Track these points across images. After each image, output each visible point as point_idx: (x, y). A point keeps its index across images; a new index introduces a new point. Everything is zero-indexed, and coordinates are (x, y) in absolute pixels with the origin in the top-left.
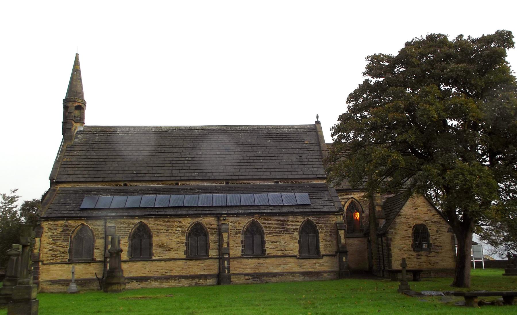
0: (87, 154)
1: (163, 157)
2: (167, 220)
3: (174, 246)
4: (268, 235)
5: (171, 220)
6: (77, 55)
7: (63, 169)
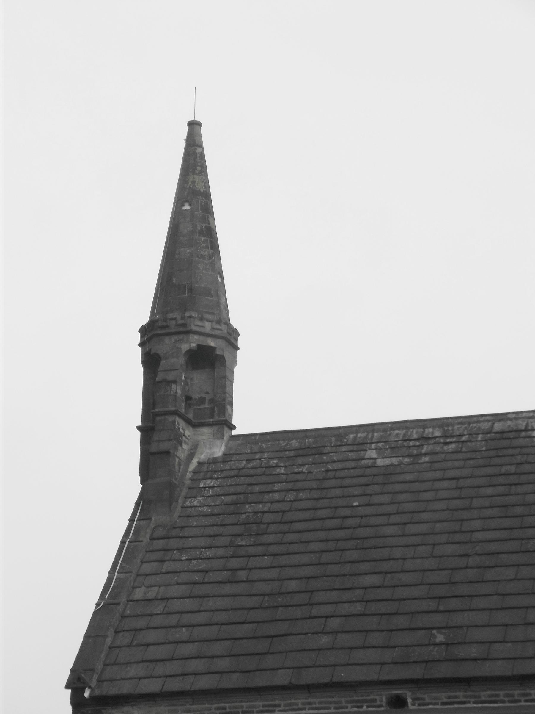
0: (234, 563)
6: (194, 126)
7: (124, 639)
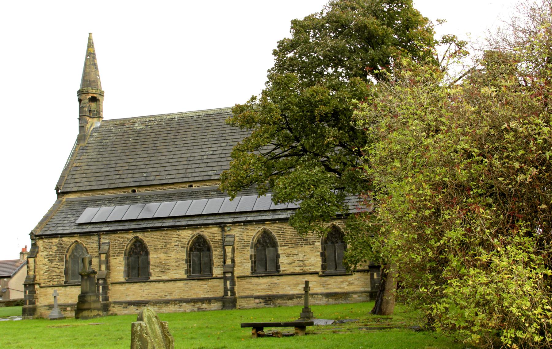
0: (99, 156)
1: (180, 152)
2: (164, 233)
3: (174, 264)
4: (283, 248)
5: (169, 233)
7: (70, 177)
